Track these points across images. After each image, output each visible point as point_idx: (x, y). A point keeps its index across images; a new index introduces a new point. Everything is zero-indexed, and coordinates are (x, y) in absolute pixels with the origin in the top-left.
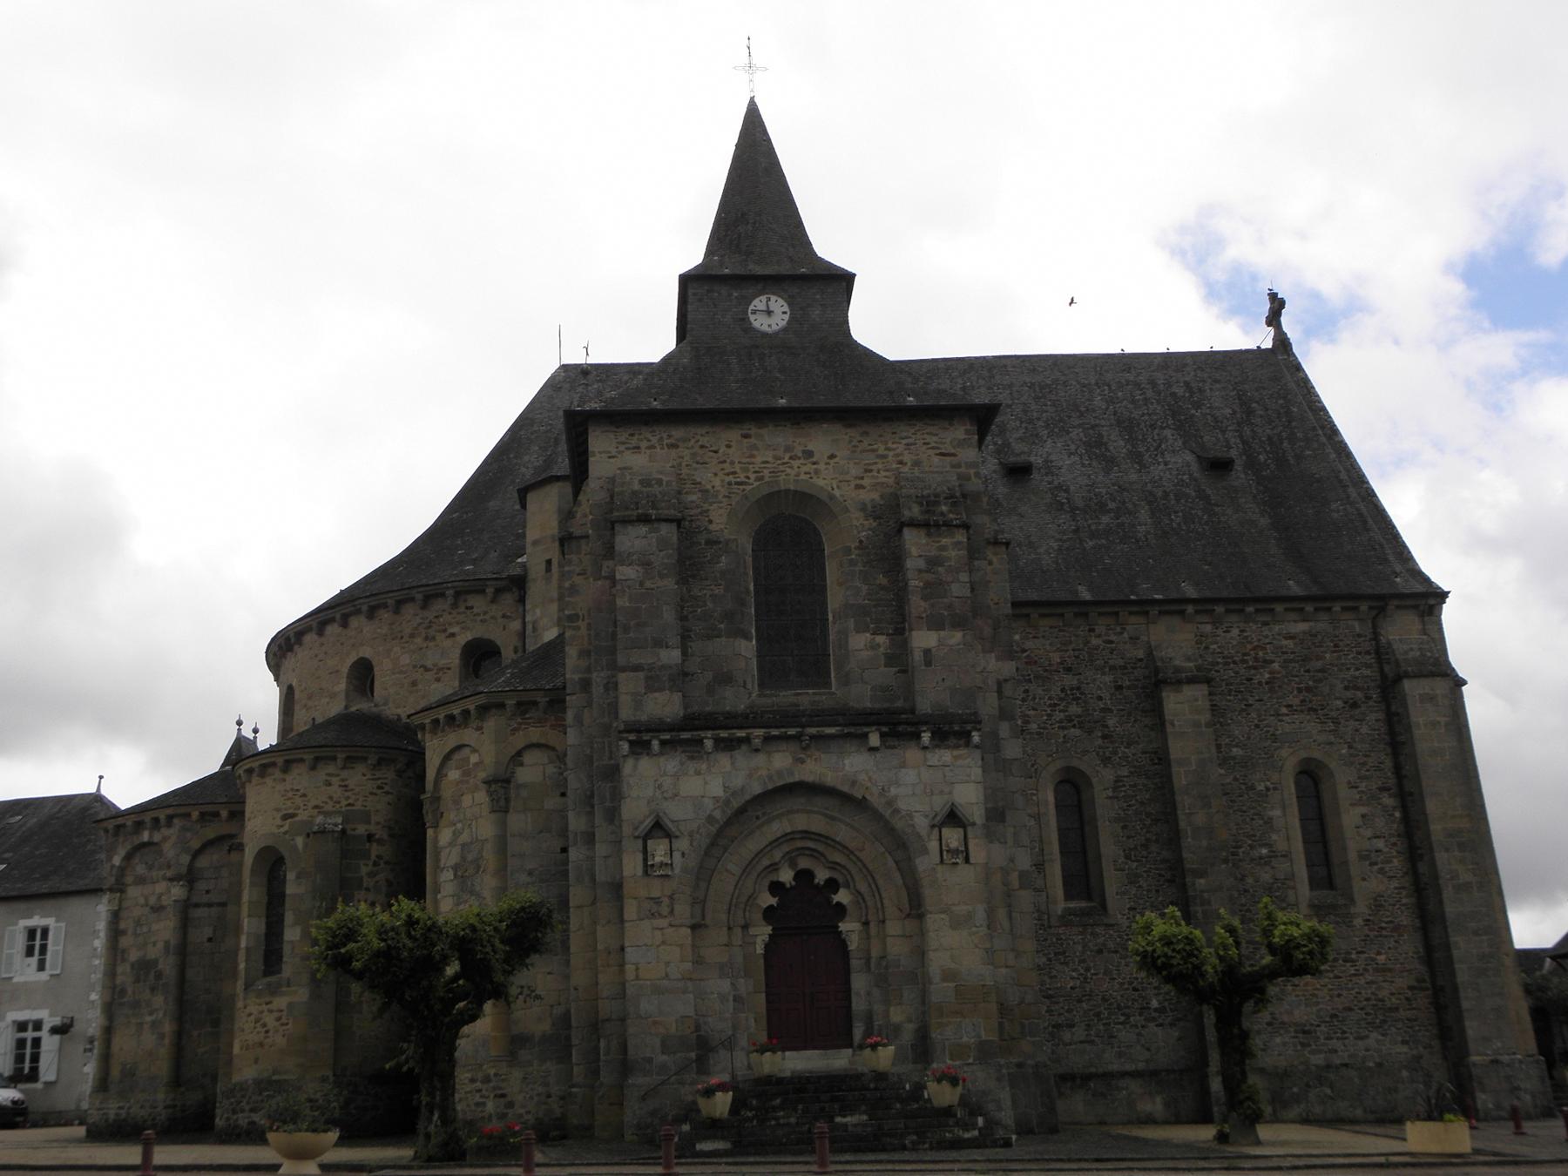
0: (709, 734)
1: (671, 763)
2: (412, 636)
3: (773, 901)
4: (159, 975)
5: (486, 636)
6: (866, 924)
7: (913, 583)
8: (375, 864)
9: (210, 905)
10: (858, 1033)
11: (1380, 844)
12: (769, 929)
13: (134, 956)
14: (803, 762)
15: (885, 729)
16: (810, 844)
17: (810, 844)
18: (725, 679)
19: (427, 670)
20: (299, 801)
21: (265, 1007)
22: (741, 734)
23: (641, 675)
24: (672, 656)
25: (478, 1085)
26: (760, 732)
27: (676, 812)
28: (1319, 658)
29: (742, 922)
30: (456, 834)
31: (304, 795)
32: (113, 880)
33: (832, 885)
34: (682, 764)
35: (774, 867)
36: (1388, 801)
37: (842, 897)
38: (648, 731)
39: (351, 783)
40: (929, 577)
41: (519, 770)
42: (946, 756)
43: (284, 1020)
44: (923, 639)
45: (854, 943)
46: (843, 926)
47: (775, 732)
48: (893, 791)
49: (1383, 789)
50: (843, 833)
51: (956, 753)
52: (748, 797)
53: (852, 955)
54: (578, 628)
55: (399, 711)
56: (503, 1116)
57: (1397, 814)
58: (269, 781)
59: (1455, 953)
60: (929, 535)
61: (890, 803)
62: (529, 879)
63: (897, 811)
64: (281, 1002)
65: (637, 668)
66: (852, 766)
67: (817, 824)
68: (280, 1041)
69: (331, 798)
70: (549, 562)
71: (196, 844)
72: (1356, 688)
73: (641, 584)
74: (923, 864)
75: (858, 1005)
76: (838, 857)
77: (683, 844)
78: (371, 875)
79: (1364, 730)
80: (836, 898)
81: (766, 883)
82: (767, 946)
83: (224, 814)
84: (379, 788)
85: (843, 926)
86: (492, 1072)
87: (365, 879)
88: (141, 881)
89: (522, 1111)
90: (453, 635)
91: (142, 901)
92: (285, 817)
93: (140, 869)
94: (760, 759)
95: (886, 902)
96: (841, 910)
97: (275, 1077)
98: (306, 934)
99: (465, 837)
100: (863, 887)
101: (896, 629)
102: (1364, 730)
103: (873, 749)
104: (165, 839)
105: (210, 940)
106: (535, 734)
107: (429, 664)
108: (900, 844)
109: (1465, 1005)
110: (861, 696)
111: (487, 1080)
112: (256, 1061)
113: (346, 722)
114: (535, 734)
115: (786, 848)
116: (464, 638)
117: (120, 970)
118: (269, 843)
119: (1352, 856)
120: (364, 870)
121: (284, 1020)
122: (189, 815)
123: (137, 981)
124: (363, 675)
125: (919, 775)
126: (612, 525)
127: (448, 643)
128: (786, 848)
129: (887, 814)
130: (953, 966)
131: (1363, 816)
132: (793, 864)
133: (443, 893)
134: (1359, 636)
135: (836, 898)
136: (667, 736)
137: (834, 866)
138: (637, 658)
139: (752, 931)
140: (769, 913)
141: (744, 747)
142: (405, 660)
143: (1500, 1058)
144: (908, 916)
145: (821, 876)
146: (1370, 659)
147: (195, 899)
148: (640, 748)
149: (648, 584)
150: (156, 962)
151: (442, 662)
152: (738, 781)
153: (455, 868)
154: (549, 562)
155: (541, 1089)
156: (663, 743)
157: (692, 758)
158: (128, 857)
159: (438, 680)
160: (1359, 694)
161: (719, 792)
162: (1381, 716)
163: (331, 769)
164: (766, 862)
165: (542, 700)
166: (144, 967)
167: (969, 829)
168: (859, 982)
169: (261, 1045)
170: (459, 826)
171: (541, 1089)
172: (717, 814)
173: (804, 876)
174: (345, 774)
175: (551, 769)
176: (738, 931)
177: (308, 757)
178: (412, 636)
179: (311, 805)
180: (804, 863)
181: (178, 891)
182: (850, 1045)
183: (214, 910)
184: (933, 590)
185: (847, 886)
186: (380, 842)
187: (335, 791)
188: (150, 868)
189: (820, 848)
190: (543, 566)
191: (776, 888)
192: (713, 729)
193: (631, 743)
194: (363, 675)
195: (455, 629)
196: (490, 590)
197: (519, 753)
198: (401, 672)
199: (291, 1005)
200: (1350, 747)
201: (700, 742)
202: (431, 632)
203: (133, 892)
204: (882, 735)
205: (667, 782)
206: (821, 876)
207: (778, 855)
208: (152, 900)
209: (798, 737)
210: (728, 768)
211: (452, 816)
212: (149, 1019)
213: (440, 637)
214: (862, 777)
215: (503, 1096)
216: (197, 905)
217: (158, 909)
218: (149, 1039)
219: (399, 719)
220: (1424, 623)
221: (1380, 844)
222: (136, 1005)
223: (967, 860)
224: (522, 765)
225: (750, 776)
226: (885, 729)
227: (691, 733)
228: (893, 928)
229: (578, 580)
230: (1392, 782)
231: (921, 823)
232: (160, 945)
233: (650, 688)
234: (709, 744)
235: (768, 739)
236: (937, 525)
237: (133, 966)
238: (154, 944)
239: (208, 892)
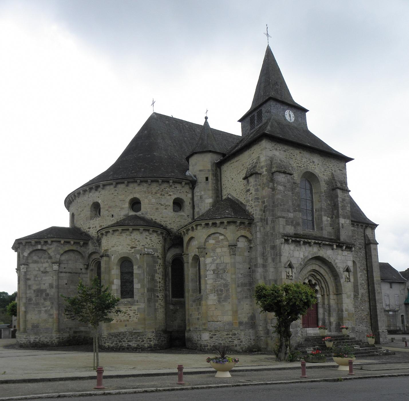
0: (303, 240)
1: (292, 247)
2: (156, 193)
4: (47, 295)
5: (181, 198)
6: (323, 296)
7: (340, 205)
8: (159, 266)
9: (66, 273)
10: (320, 324)
11: (363, 282)
13: (35, 287)
14: (320, 251)
15: (337, 244)
18: (298, 224)
19: (162, 205)
20: (137, 243)
21: (129, 309)
22: (310, 241)
23: (285, 219)
24: (291, 215)
25: (231, 336)
26: (313, 241)
27: (294, 262)
28: (355, 236)
30: (214, 260)
31: (139, 241)
32: (24, 261)
34: (294, 247)
36: (365, 272)
37: (317, 288)
38: (290, 237)
39: (153, 239)
40: (343, 204)
41: (238, 243)
42: (345, 253)
43: (136, 313)
44: (342, 221)
47: (317, 241)
48: (337, 261)
49: (364, 269)
50: (322, 271)
51: (348, 253)
52: (308, 259)
54: (259, 202)
55: (152, 217)
56: (240, 345)
57: (366, 275)
58: (124, 235)
59: (377, 307)
60: (342, 192)
61: (336, 264)
62: (241, 276)
63: (337, 266)
64: (135, 307)
65: (283, 217)
66: (327, 253)
67: (317, 268)
68: (136, 320)
69: (147, 243)
70: (207, 179)
71: (62, 252)
72: (361, 245)
73: (284, 192)
74: (342, 281)
75: (320, 316)
76: (318, 277)
77: (294, 270)
78: (159, 269)
79: (362, 255)
83: (72, 242)
84: (159, 241)
86: (236, 332)
87: (158, 270)
88: (36, 262)
89: (244, 344)
90: (170, 195)
91: (37, 269)
92: (132, 248)
93: (35, 258)
94: (310, 249)
95: (330, 290)
96: (316, 291)
97: (134, 331)
98: (143, 286)
99: (218, 261)
100: (324, 286)
101: (332, 217)
102: (362, 255)
103: (333, 249)
104: (49, 249)
105: (66, 284)
106: (243, 232)
107: (163, 203)
108: (335, 275)
109: (379, 319)
110: (325, 234)
111: (235, 334)
112: (126, 326)
113: (128, 218)
114: (243, 232)
116: (174, 197)
117: (28, 292)
118: (126, 256)
119: (359, 284)
120: (157, 267)
121: (136, 313)
122: (60, 242)
123: (37, 296)
124: (135, 204)
125: (341, 258)
126: (273, 173)
127: (169, 197)
129: (335, 267)
130: (347, 308)
131: (361, 275)
132: (308, 278)
133: (208, 277)
134: (362, 232)
136: (294, 239)
137: (317, 280)
138: (284, 214)
141: (308, 245)
142: (153, 201)
143: (384, 331)
144: (335, 294)
145: (314, 282)
146: (363, 238)
147: (61, 270)
148: (287, 241)
149: (286, 192)
150: (45, 290)
151: (167, 204)
152: (306, 254)
153: (214, 271)
154: (207, 179)
155: (249, 337)
156: (292, 241)
157: (296, 246)
158: (30, 254)
159: (166, 209)
160: (361, 246)
161: (302, 256)
162: (365, 252)
163: (147, 233)
165: (247, 222)
166: (39, 292)
167: (350, 273)
168: (321, 311)
169: (128, 321)
170: (215, 258)
171: (249, 337)
172: (302, 263)
173: (310, 281)
174: (151, 236)
175: (246, 244)
177: (131, 229)
178: (156, 193)
179: (141, 244)
180: (310, 278)
181: (56, 267)
183: (67, 274)
184: (344, 207)
186: (160, 259)
187: (148, 240)
188: (40, 258)
189: (315, 274)
190: (205, 179)
192: (304, 239)
193: (285, 240)
194: (135, 204)
195: (171, 193)
196: (184, 183)
197: (238, 238)
198: (152, 204)
199: (138, 309)
200: (359, 259)
201: (299, 242)
202: (163, 193)
203: (32, 266)
204: (337, 246)
205: (291, 252)
208: (42, 269)
209: (319, 244)
210: (304, 250)
211: (212, 254)
212: (44, 309)
213: (166, 195)
214: (330, 256)
215: (240, 339)
216: (61, 272)
217: (45, 272)
218: (44, 316)
219: (152, 220)
220: (372, 231)
221: (363, 282)
222: (37, 304)
223: (350, 281)
224: (238, 241)
225: (309, 253)
226: (337, 244)
227: (296, 239)
228: (332, 297)
229: (259, 187)
230: (366, 267)
231: (341, 270)
232: (47, 285)
233: (287, 224)
234: (302, 242)
235: (315, 243)
236: (344, 190)
237: (34, 291)
238: (44, 284)
239: (65, 268)
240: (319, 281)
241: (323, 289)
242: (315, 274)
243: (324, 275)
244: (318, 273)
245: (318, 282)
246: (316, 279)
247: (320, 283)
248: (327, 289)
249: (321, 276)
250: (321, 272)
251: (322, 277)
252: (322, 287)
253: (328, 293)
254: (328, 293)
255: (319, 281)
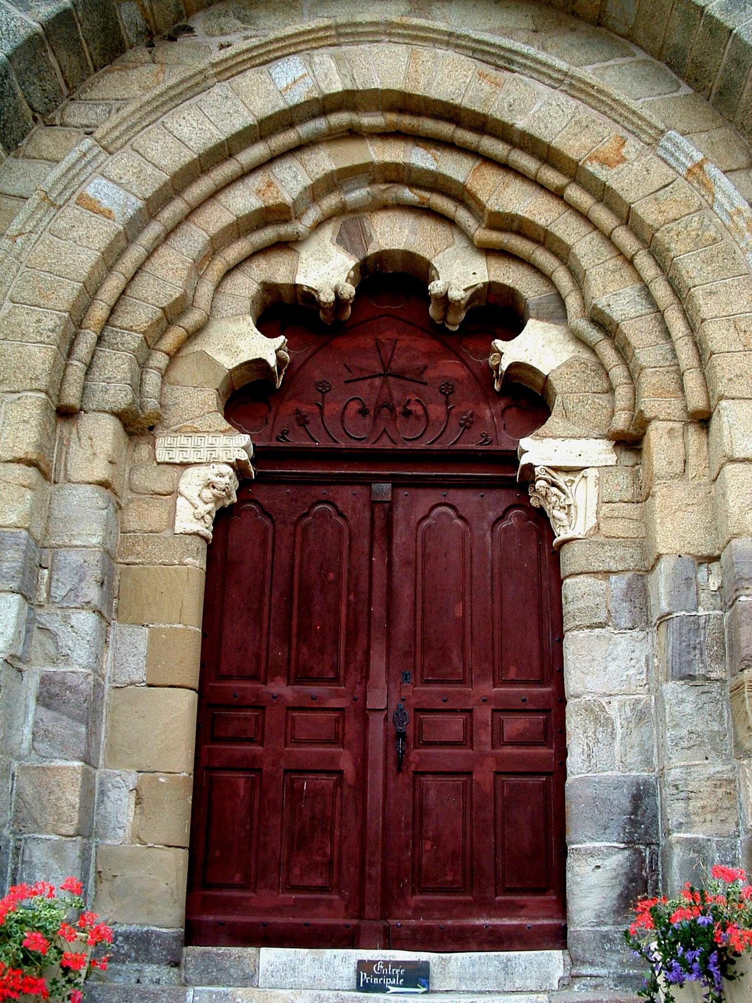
3: (268, 349)
6: (630, 442)
10: (593, 877)
12: (238, 445)
16: (421, 158)
17: (421, 158)
29: (119, 395)
33: (499, 312)
35: (274, 229)
45: (578, 514)
46: (536, 450)
53: (570, 560)
75: (595, 762)
80: (511, 352)
81: (245, 287)
82: (224, 518)
85: (536, 450)
96: (530, 398)
100: (620, 301)
115: (324, 161)
128: (324, 161)
135: (511, 352)
139: (167, 447)
140: (246, 395)
145: (458, 273)
164: (244, 200)
176: (100, 433)
180: (393, 233)
182: (557, 937)
185: (558, 312)
189: (456, 168)
191: (280, 310)
206: (458, 273)
207: (291, 180)
240: (543, 258)
241: (623, 351)
242: (456, 168)
243: (572, 146)
244: (498, 148)
245: (547, 277)
246: (482, 234)
247: (562, 278)
248: (678, 327)
249: (552, 177)
250: (521, 123)
251: (574, 193)
252: (601, 322)
253: (692, 381)
254: (692, 381)
255: (543, 258)
